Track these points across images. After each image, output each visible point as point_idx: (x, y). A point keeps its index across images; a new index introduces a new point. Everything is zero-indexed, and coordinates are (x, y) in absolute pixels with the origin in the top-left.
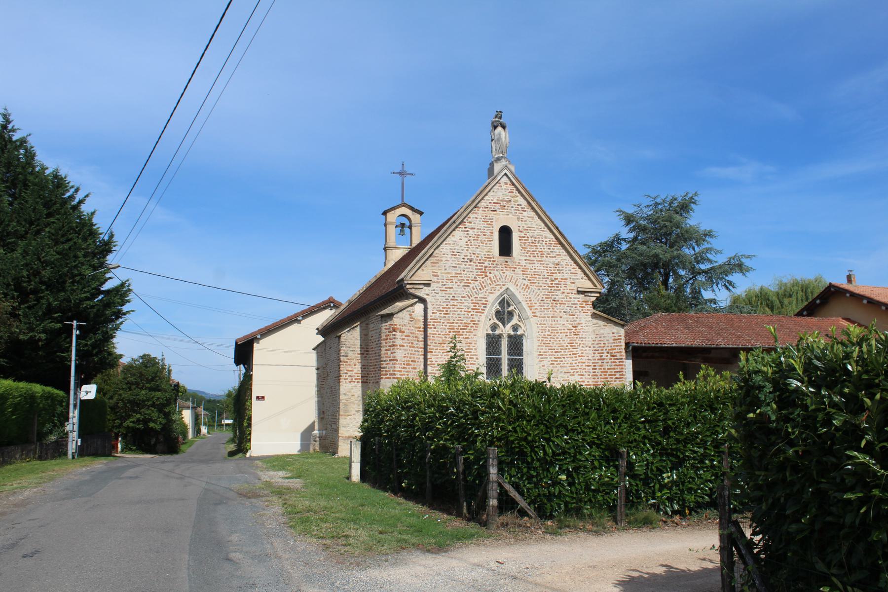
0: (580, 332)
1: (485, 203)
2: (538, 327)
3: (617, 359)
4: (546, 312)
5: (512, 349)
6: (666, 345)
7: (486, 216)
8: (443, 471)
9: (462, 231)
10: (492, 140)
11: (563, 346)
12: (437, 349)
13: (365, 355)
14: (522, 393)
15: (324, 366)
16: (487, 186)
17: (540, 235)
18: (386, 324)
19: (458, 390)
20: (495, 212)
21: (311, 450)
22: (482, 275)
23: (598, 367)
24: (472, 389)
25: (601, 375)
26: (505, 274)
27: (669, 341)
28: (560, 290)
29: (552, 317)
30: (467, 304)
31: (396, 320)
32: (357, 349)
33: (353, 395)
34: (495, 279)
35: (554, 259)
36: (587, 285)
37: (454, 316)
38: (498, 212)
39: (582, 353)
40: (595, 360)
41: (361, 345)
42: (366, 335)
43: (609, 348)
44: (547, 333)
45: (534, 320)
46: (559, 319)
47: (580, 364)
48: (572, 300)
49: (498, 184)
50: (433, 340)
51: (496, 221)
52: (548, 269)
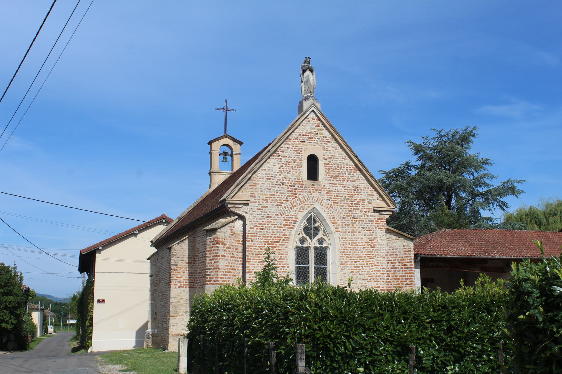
0: (375, 245)
1: (296, 135)
2: (340, 241)
3: (407, 268)
4: (347, 228)
5: (318, 259)
6: (449, 256)
7: (296, 146)
8: (259, 364)
9: (276, 159)
10: (302, 82)
11: (361, 257)
12: (254, 259)
13: (192, 264)
14: (326, 297)
15: (157, 273)
16: (297, 121)
17: (342, 163)
18: (211, 238)
19: (271, 294)
20: (304, 143)
21: (145, 346)
22: (293, 196)
23: (391, 275)
24: (283, 294)
25: (393, 282)
26: (312, 196)
27: (451, 253)
28: (358, 209)
29: (352, 232)
30: (280, 221)
31: (219, 234)
32: (185, 259)
33: (181, 299)
34: (304, 200)
35: (354, 183)
36: (382, 205)
37: (268, 231)
38: (306, 143)
39: (378, 263)
40: (389, 268)
41: (189, 256)
42: (194, 247)
43: (401, 258)
45: (336, 235)
46: (358, 234)
47: (375, 272)
48: (369, 217)
49: (306, 119)
50: (250, 251)
51: (305, 150)
52: (349, 191)
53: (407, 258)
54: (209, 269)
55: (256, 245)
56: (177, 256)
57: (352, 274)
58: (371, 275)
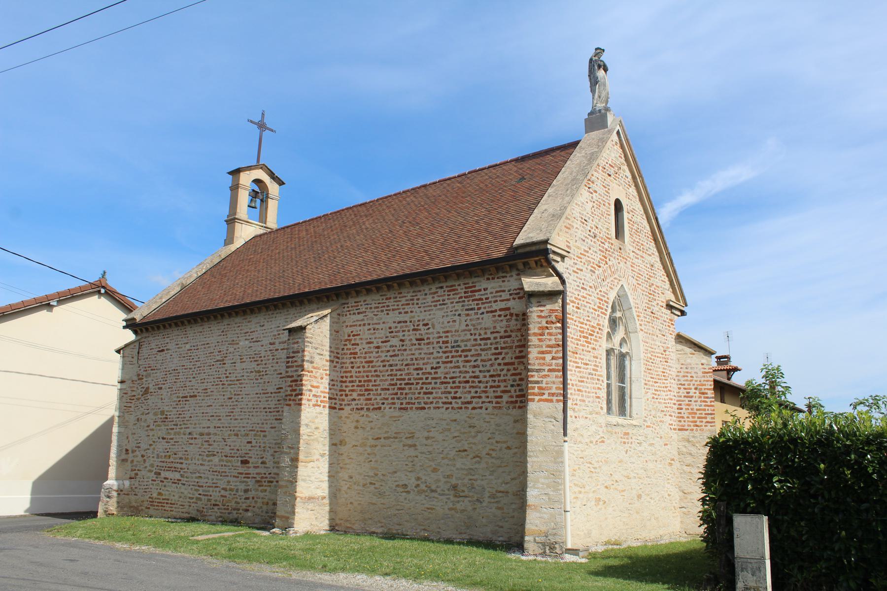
0: (668, 359)
3: (707, 398)
15: (135, 378)
22: (603, 260)
25: (688, 417)
28: (655, 300)
30: (593, 298)
33: (317, 428)
35: (650, 258)
40: (681, 397)
41: (330, 347)
42: (338, 332)
43: (698, 383)
44: (649, 355)
45: (641, 334)
52: (647, 269)
53: (707, 383)
54: (538, 371)
55: (573, 336)
56: (314, 345)
57: (653, 400)
58: (666, 405)
